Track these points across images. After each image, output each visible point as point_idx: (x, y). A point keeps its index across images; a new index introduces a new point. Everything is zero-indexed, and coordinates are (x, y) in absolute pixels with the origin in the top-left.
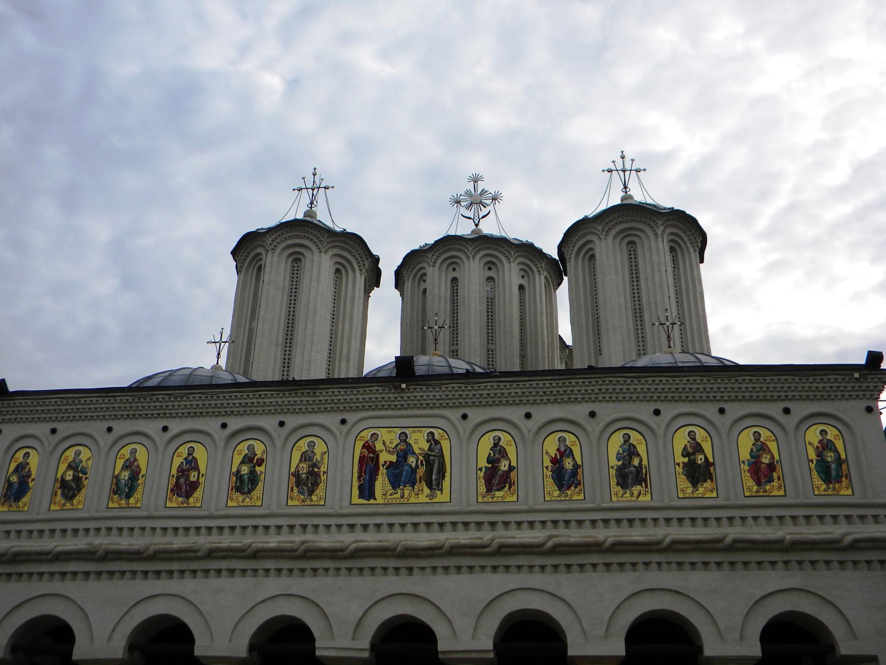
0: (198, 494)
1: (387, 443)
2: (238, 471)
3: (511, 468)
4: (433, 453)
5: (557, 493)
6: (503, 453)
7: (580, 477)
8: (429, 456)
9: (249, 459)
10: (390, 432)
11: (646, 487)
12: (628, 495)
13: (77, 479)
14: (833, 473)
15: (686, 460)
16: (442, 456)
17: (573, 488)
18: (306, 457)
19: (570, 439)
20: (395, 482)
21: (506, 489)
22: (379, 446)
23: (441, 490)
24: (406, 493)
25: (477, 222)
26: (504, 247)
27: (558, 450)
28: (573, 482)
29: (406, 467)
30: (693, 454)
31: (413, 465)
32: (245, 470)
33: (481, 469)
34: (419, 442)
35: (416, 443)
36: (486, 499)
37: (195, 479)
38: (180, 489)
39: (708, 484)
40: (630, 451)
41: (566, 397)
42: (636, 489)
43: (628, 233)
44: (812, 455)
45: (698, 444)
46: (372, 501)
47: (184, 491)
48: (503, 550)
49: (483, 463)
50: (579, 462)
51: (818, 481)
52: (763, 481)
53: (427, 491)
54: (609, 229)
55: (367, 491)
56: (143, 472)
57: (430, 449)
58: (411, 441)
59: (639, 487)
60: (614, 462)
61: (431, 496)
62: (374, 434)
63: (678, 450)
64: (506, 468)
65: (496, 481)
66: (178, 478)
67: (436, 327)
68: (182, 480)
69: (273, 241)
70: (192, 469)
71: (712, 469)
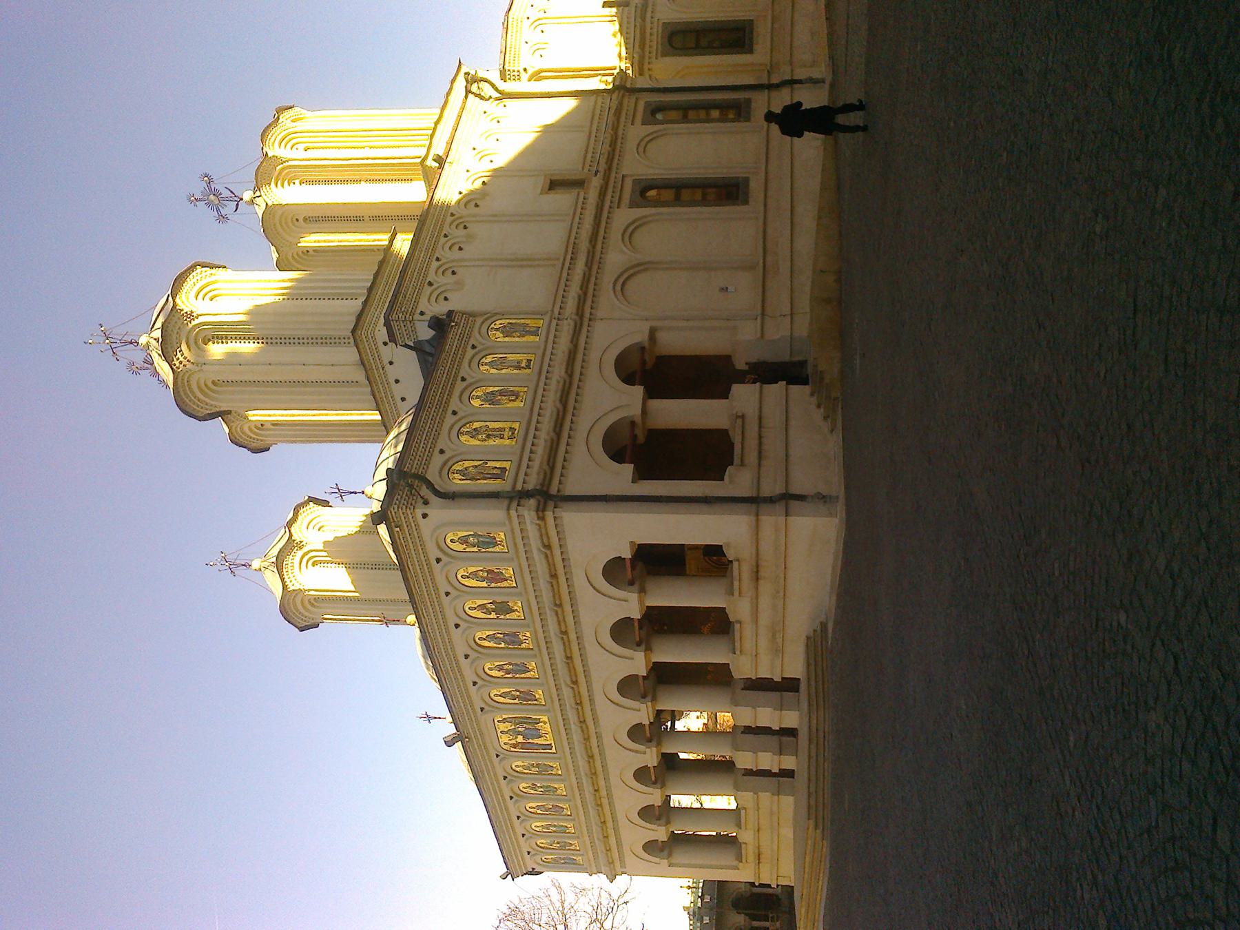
12: (527, 642)
13: (558, 843)
14: (487, 540)
22: (513, 742)
24: (544, 732)
43: (206, 390)
44: (475, 549)
46: (553, 745)
49: (516, 701)
51: (497, 549)
52: (502, 577)
54: (207, 405)
55: (549, 746)
60: (503, 645)
61: (545, 723)
63: (489, 616)
65: (529, 698)
69: (305, 621)
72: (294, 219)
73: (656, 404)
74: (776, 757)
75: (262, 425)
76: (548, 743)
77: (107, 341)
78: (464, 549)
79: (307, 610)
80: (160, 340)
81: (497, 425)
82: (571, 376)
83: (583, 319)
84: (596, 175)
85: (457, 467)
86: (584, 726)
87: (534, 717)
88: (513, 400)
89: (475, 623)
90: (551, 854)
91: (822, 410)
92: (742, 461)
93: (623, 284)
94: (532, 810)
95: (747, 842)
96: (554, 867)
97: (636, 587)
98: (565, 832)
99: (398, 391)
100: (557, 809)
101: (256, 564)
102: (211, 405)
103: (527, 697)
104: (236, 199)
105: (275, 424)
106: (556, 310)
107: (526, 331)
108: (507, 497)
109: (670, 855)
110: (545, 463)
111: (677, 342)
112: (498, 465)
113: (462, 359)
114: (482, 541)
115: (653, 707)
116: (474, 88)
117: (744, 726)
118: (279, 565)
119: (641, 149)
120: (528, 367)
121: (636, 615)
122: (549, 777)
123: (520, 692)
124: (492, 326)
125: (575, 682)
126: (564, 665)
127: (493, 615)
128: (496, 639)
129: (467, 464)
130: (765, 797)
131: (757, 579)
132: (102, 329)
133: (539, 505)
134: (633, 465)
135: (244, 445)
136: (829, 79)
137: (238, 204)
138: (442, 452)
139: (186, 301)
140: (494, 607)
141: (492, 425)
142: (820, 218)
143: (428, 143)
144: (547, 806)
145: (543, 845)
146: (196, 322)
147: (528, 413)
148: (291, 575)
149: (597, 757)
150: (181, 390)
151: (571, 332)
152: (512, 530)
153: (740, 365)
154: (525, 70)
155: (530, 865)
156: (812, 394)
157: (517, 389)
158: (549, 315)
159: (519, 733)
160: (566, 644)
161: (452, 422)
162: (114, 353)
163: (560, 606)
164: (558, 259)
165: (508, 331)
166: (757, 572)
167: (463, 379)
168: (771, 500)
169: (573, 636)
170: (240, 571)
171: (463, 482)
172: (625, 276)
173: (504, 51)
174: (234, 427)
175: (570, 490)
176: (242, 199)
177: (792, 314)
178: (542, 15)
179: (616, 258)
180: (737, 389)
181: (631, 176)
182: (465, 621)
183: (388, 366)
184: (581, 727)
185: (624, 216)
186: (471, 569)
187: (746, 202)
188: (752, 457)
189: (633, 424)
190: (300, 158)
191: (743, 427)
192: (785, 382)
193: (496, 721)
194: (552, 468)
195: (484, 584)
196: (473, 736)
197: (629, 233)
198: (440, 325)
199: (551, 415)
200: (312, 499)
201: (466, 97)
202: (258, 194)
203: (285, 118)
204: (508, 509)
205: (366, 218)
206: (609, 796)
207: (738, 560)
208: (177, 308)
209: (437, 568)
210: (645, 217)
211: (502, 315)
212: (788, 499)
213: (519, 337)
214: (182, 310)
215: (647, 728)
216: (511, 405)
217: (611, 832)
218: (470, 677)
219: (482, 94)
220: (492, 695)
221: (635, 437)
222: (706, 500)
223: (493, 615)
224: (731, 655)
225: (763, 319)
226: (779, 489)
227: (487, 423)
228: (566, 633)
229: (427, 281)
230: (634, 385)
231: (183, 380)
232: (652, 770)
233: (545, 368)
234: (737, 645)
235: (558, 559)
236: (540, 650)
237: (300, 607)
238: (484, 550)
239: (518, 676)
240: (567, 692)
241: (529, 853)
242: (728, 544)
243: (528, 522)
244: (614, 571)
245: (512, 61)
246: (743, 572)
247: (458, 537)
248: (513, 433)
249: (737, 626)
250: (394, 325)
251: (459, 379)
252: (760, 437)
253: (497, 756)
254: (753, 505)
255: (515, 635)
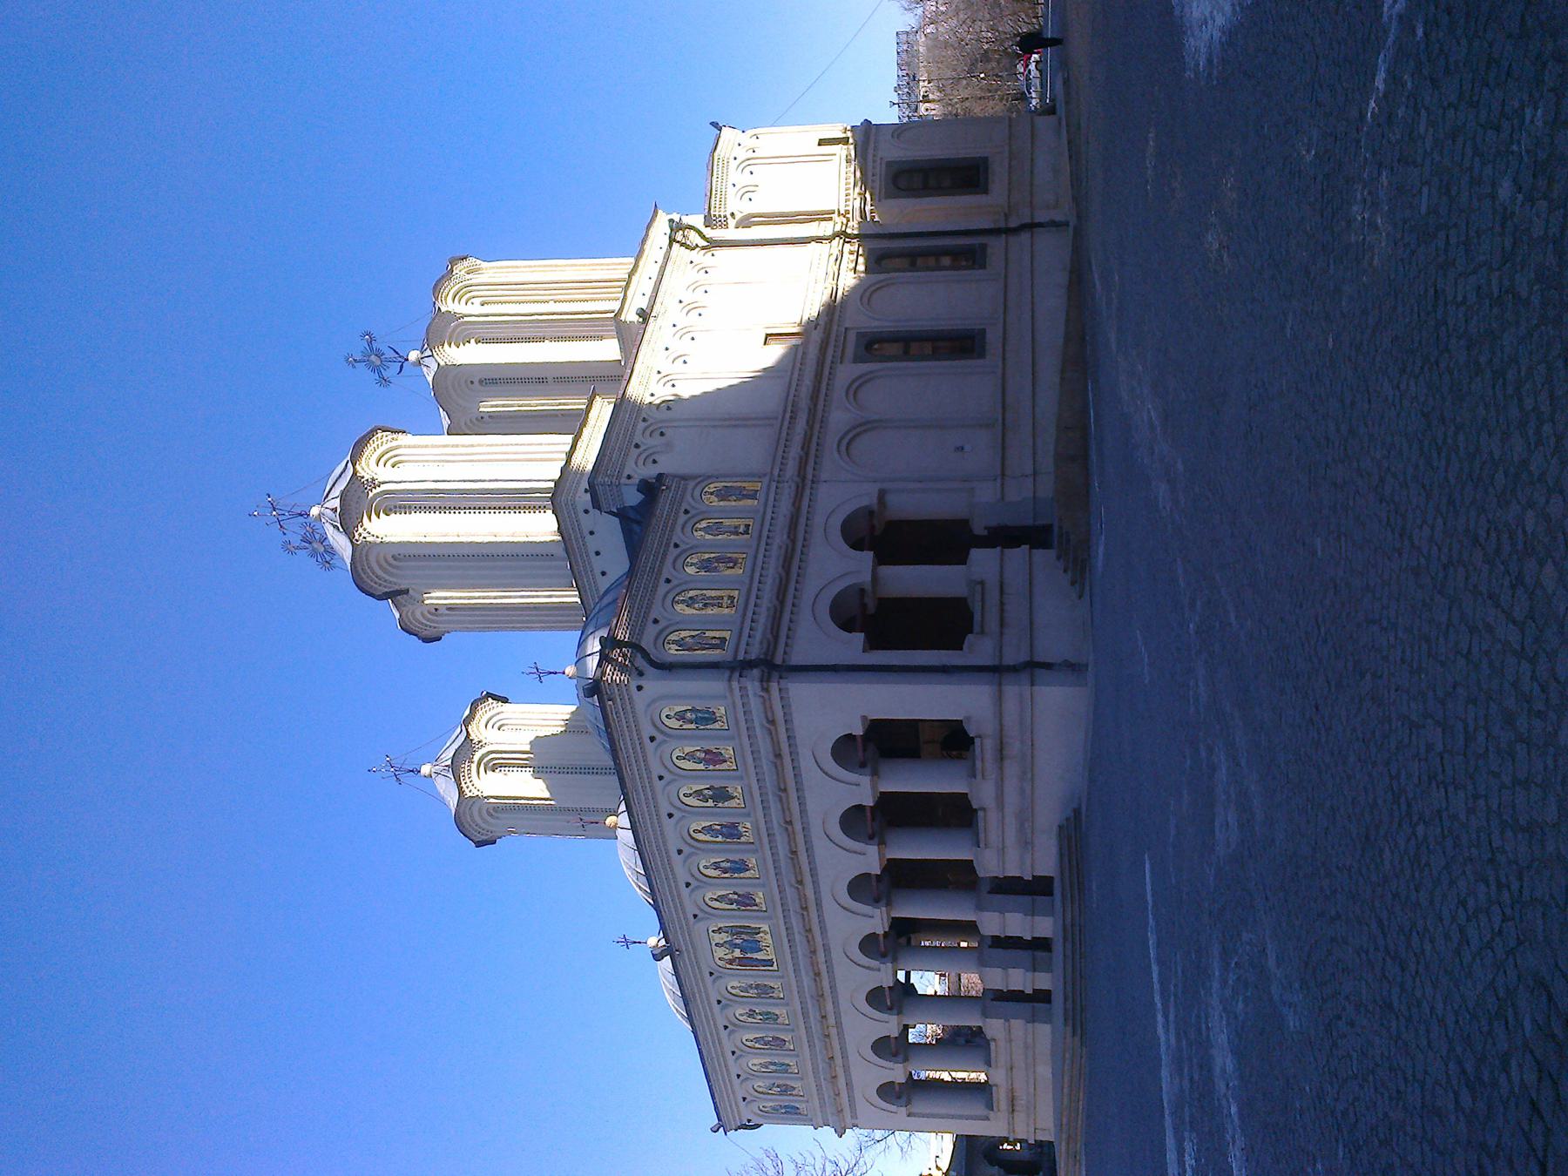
3: (735, 893)
12: (747, 834)
13: (778, 1086)
14: (706, 715)
22: (730, 957)
34: (724, 937)
43: (385, 564)
44: (693, 726)
46: (774, 960)
49: (734, 906)
51: (716, 726)
53: (761, 935)
55: (769, 963)
57: (727, 932)
59: (740, 828)
60: (720, 839)
61: (764, 932)
63: (706, 804)
65: (748, 902)
72: (469, 382)
73: (887, 571)
74: (1029, 974)
75: (436, 610)
76: (770, 958)
77: (274, 513)
78: (681, 726)
79: (485, 821)
80: (339, 511)
81: (713, 593)
82: (794, 542)
83: (804, 482)
84: (816, 328)
85: (673, 637)
86: (810, 937)
87: (753, 926)
88: (731, 568)
89: (689, 812)
90: (771, 1100)
91: (1069, 573)
92: (982, 627)
93: (849, 444)
94: (748, 1044)
95: (999, 1084)
96: (773, 1118)
97: (868, 770)
98: (786, 1072)
99: (598, 564)
100: (778, 1042)
101: (426, 769)
102: (390, 582)
103: (746, 901)
104: (400, 359)
105: (450, 608)
106: (776, 472)
107: (742, 494)
108: (728, 668)
109: (908, 1103)
110: (769, 631)
111: (911, 504)
112: (717, 634)
113: (674, 525)
114: (702, 718)
115: (888, 914)
116: (679, 236)
117: (992, 936)
118: (455, 768)
119: (865, 300)
120: (746, 532)
121: (869, 802)
122: (768, 1001)
123: (739, 896)
124: (706, 489)
125: (801, 882)
126: (789, 861)
127: (710, 804)
129: (684, 634)
130: (1017, 1025)
131: (1002, 759)
132: (270, 499)
133: (763, 675)
134: (861, 636)
135: (415, 632)
136: (1073, 221)
137: (402, 367)
138: (656, 621)
139: (369, 467)
140: (711, 793)
141: (709, 593)
142: (1062, 371)
143: (622, 295)
144: (766, 1039)
145: (760, 1090)
146: (378, 490)
147: (747, 581)
148: (468, 780)
149: (824, 974)
150: (359, 569)
151: (793, 495)
152: (734, 703)
153: (979, 529)
154: (732, 214)
155: (747, 1113)
156: (1059, 558)
157: (736, 555)
158: (767, 478)
159: (736, 946)
160: (791, 836)
161: (666, 590)
162: (281, 527)
163: (785, 790)
164: (776, 418)
165: (723, 494)
166: (1001, 750)
167: (676, 546)
168: (1014, 669)
169: (798, 826)
170: (407, 778)
171: (681, 652)
172: (850, 435)
173: (709, 194)
174: (405, 612)
175: (797, 659)
176: (407, 360)
177: (1035, 474)
178: (750, 154)
179: (839, 417)
180: (976, 554)
181: (852, 329)
182: (679, 809)
183: (588, 537)
184: (807, 937)
185: (847, 372)
186: (688, 749)
187: (982, 355)
188: (992, 624)
189: (862, 590)
190: (476, 313)
191: (983, 594)
192: (1028, 546)
193: (710, 931)
194: (776, 638)
195: (701, 766)
196: (684, 949)
197: (854, 389)
198: (650, 489)
199: (774, 581)
200: (489, 695)
201: (670, 246)
202: (428, 353)
203: (460, 269)
204: (730, 680)
205: (549, 380)
206: (839, 1025)
207: (980, 737)
208: (358, 475)
209: (650, 746)
210: (871, 372)
211: (717, 478)
212: (1032, 668)
213: (735, 501)
214: (363, 477)
215: (881, 938)
216: (729, 572)
217: (840, 1071)
218: (682, 876)
219: (688, 243)
220: (707, 899)
221: (864, 606)
222: (945, 670)
223: (710, 804)
224: (974, 849)
225: (1003, 479)
226: (1023, 657)
227: (704, 592)
228: (790, 823)
229: (634, 444)
230: (862, 551)
231: (361, 554)
232: (887, 993)
233: (765, 533)
234: (982, 836)
235: (783, 736)
236: (761, 843)
237: (477, 818)
238: (702, 727)
239: (736, 875)
240: (790, 893)
241: (744, 1099)
242: (968, 718)
243: (750, 693)
244: (845, 750)
245: (718, 206)
246: (986, 748)
248: (732, 602)
249: (980, 814)
250: (600, 490)
251: (672, 545)
252: (1002, 603)
253: (711, 974)
254: (997, 675)
255: (734, 826)
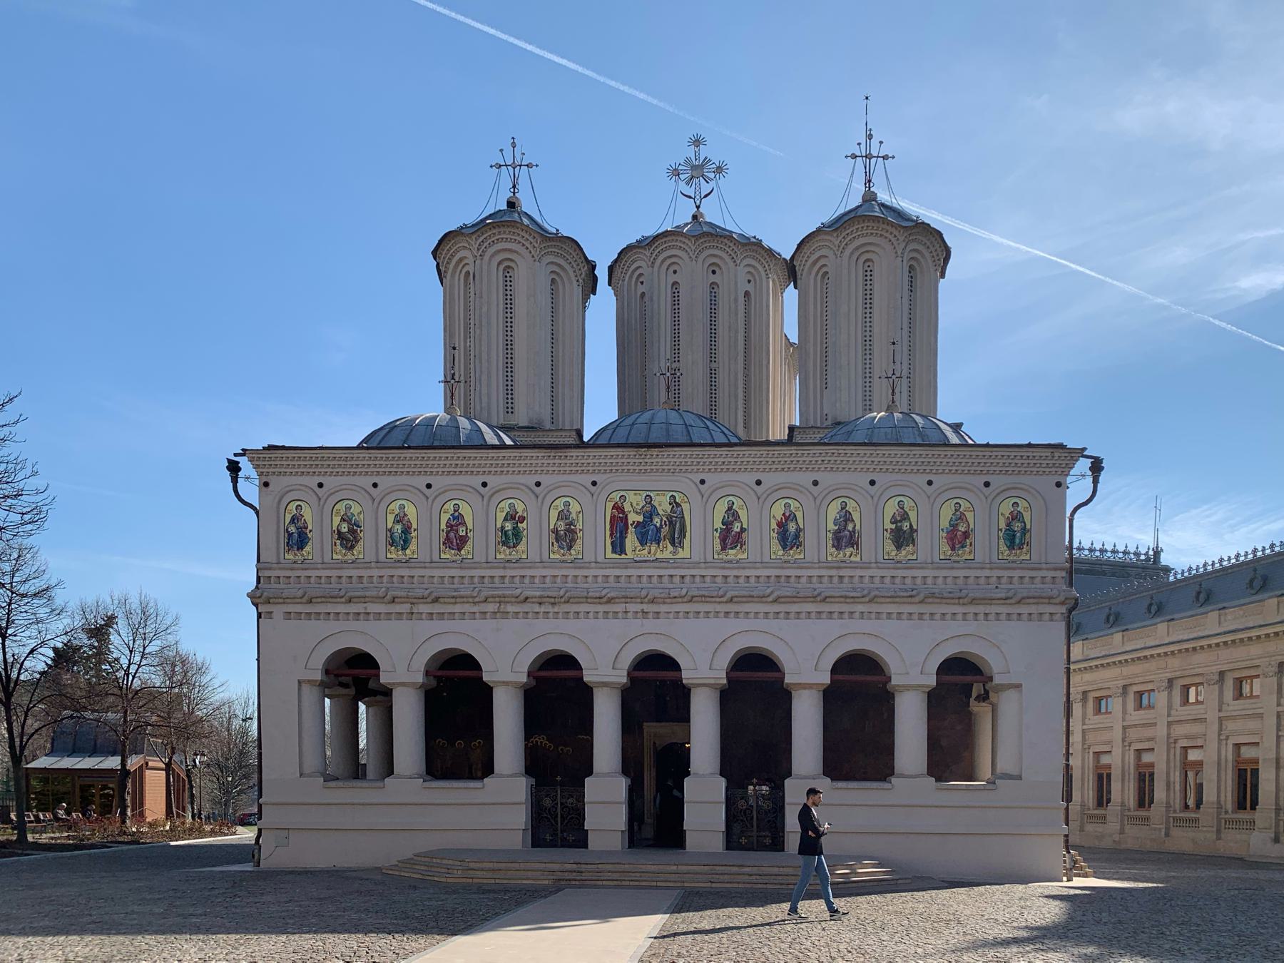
0: (468, 547)
1: (634, 505)
2: (503, 527)
3: (743, 530)
4: (675, 515)
5: (781, 552)
6: (736, 517)
7: (801, 540)
8: (671, 517)
9: (511, 516)
10: (635, 494)
11: (857, 549)
12: (841, 555)
15: (893, 526)
16: (683, 517)
17: (795, 548)
18: (563, 515)
19: (794, 505)
20: (643, 540)
21: (738, 548)
22: (627, 507)
23: (683, 548)
24: (653, 549)
25: (698, 202)
26: (730, 247)
27: (784, 515)
28: (795, 544)
29: (652, 527)
30: (900, 521)
31: (658, 525)
32: (508, 526)
33: (716, 530)
34: (663, 504)
35: (660, 505)
36: (721, 556)
37: (462, 533)
38: (452, 543)
39: (910, 548)
40: (846, 517)
41: (792, 466)
42: (849, 550)
45: (906, 512)
46: (623, 556)
47: (455, 544)
48: (735, 599)
49: (718, 525)
50: (802, 527)
53: (670, 548)
55: (619, 547)
56: (414, 526)
58: (655, 503)
59: (851, 549)
62: (622, 496)
64: (738, 530)
65: (729, 541)
66: (448, 533)
67: (668, 374)
68: (452, 535)
70: (460, 524)
71: (915, 534)
128: (846, 521)
140: (906, 526)
247: (1022, 511)
249: (886, 785)
